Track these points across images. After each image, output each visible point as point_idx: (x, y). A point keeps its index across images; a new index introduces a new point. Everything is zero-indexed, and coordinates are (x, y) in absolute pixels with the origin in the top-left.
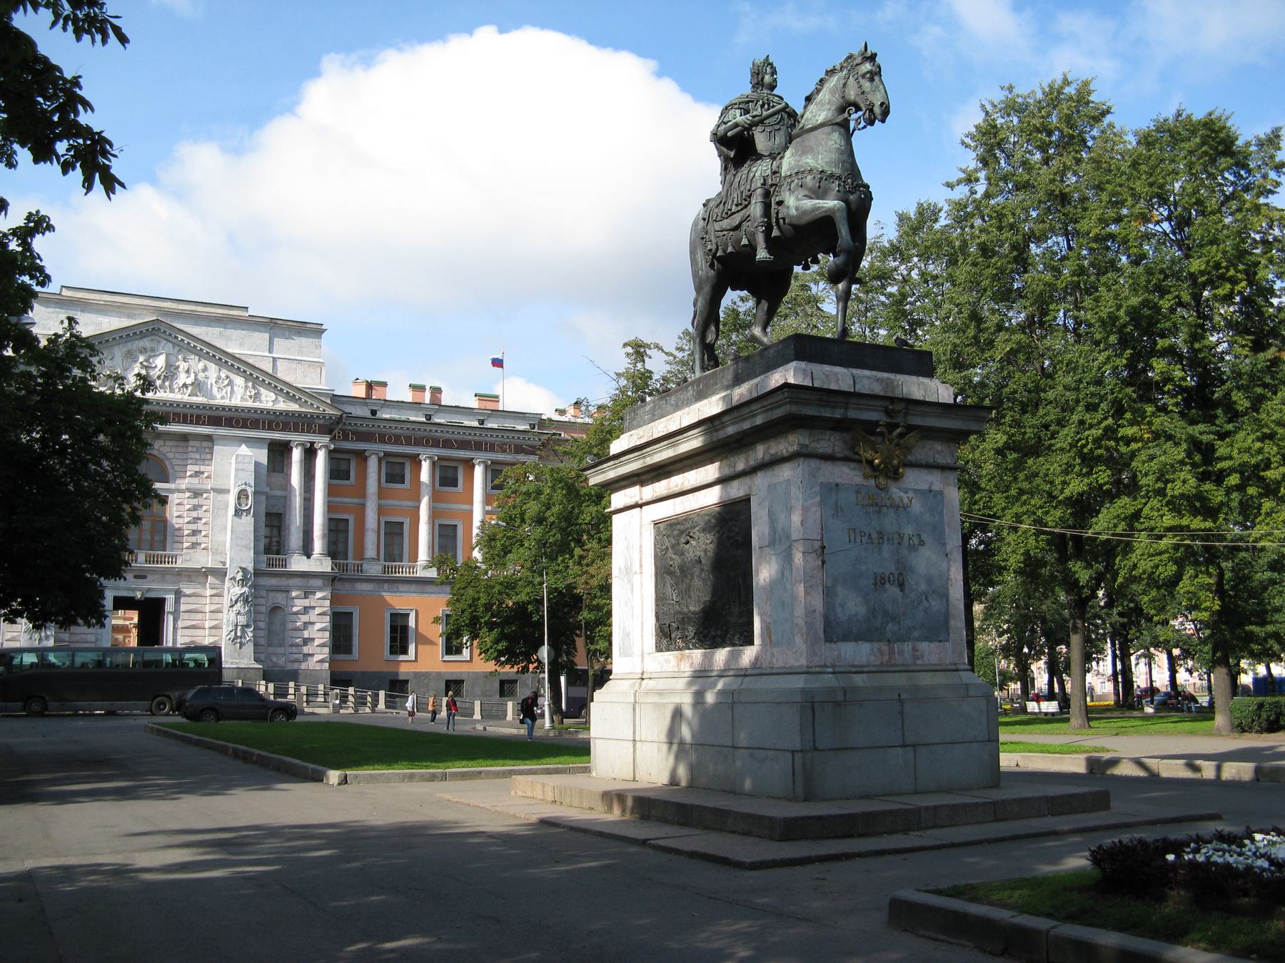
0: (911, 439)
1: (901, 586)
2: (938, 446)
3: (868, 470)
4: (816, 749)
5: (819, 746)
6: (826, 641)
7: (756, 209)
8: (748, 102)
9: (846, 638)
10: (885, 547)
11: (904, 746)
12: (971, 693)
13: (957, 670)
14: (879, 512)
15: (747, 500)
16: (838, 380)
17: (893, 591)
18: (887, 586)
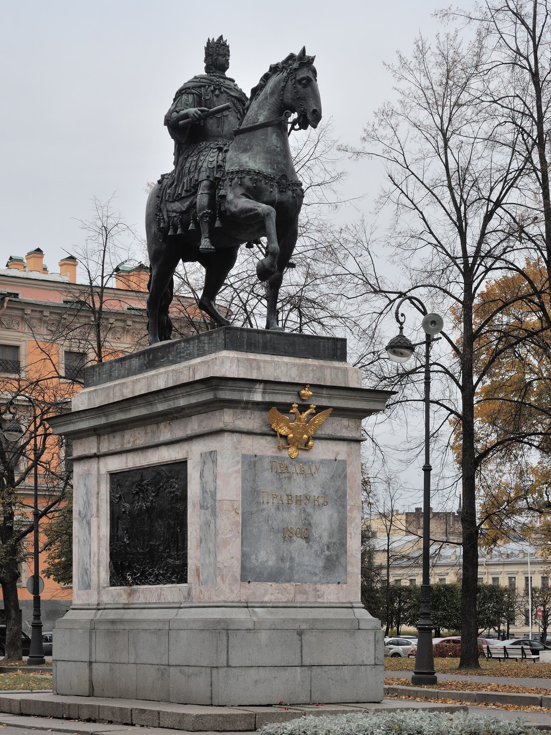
0: (319, 418)
1: (307, 539)
2: (345, 422)
3: (282, 442)
4: (228, 666)
5: (233, 663)
6: (241, 581)
7: (202, 198)
8: (200, 87)
9: (259, 578)
10: (293, 506)
11: (302, 666)
12: (362, 626)
13: (352, 608)
14: (290, 478)
15: (183, 463)
16: (259, 368)
17: (299, 542)
18: (294, 538)
